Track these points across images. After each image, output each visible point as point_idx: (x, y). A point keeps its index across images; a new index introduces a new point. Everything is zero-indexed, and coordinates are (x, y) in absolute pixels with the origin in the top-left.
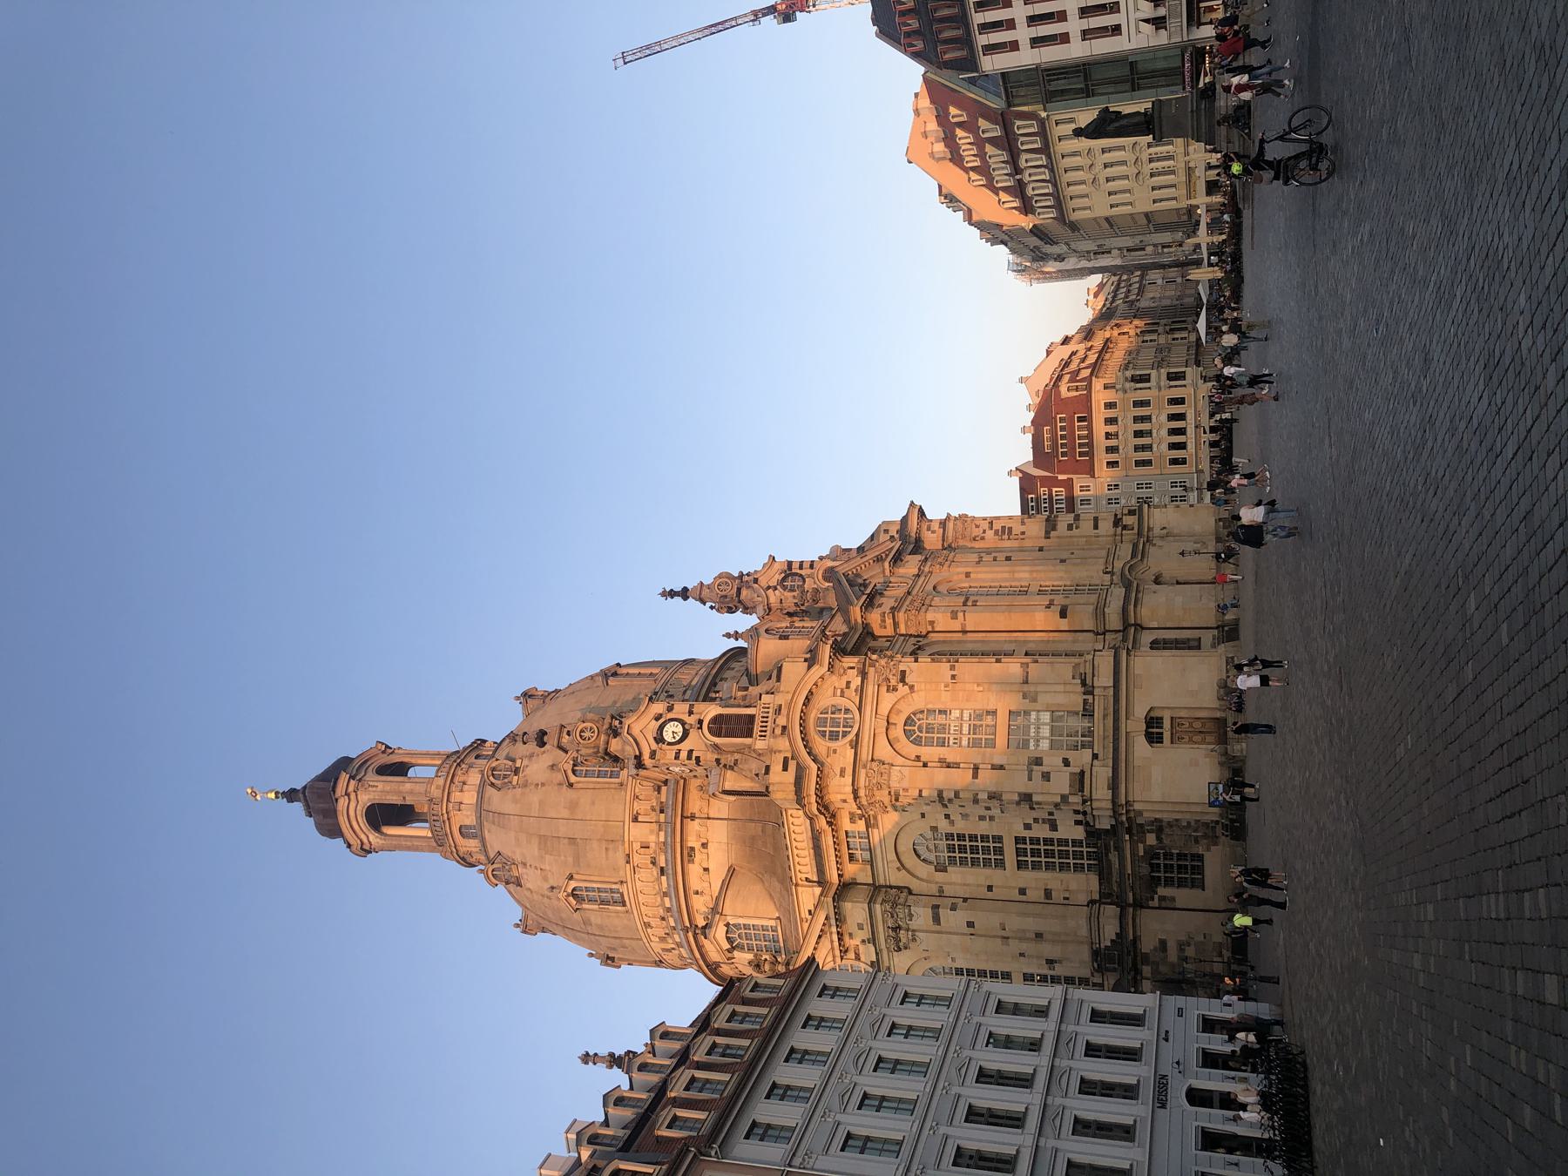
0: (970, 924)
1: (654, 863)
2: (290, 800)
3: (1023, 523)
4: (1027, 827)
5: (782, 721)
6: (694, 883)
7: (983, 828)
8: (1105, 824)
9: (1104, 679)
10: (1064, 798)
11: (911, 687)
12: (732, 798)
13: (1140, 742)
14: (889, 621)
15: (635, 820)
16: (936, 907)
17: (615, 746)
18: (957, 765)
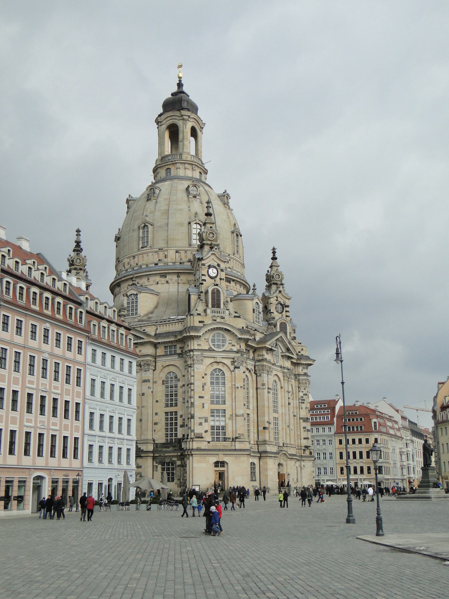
0: (143, 394)
1: (159, 260)
3: (306, 408)
4: (181, 416)
5: (218, 320)
6: (152, 279)
7: (180, 399)
8: (183, 446)
9: (238, 446)
10: (194, 430)
11: (233, 371)
12: (187, 298)
13: (215, 459)
14: (260, 358)
15: (177, 252)
16: (148, 381)
17: (207, 248)
18: (203, 390)
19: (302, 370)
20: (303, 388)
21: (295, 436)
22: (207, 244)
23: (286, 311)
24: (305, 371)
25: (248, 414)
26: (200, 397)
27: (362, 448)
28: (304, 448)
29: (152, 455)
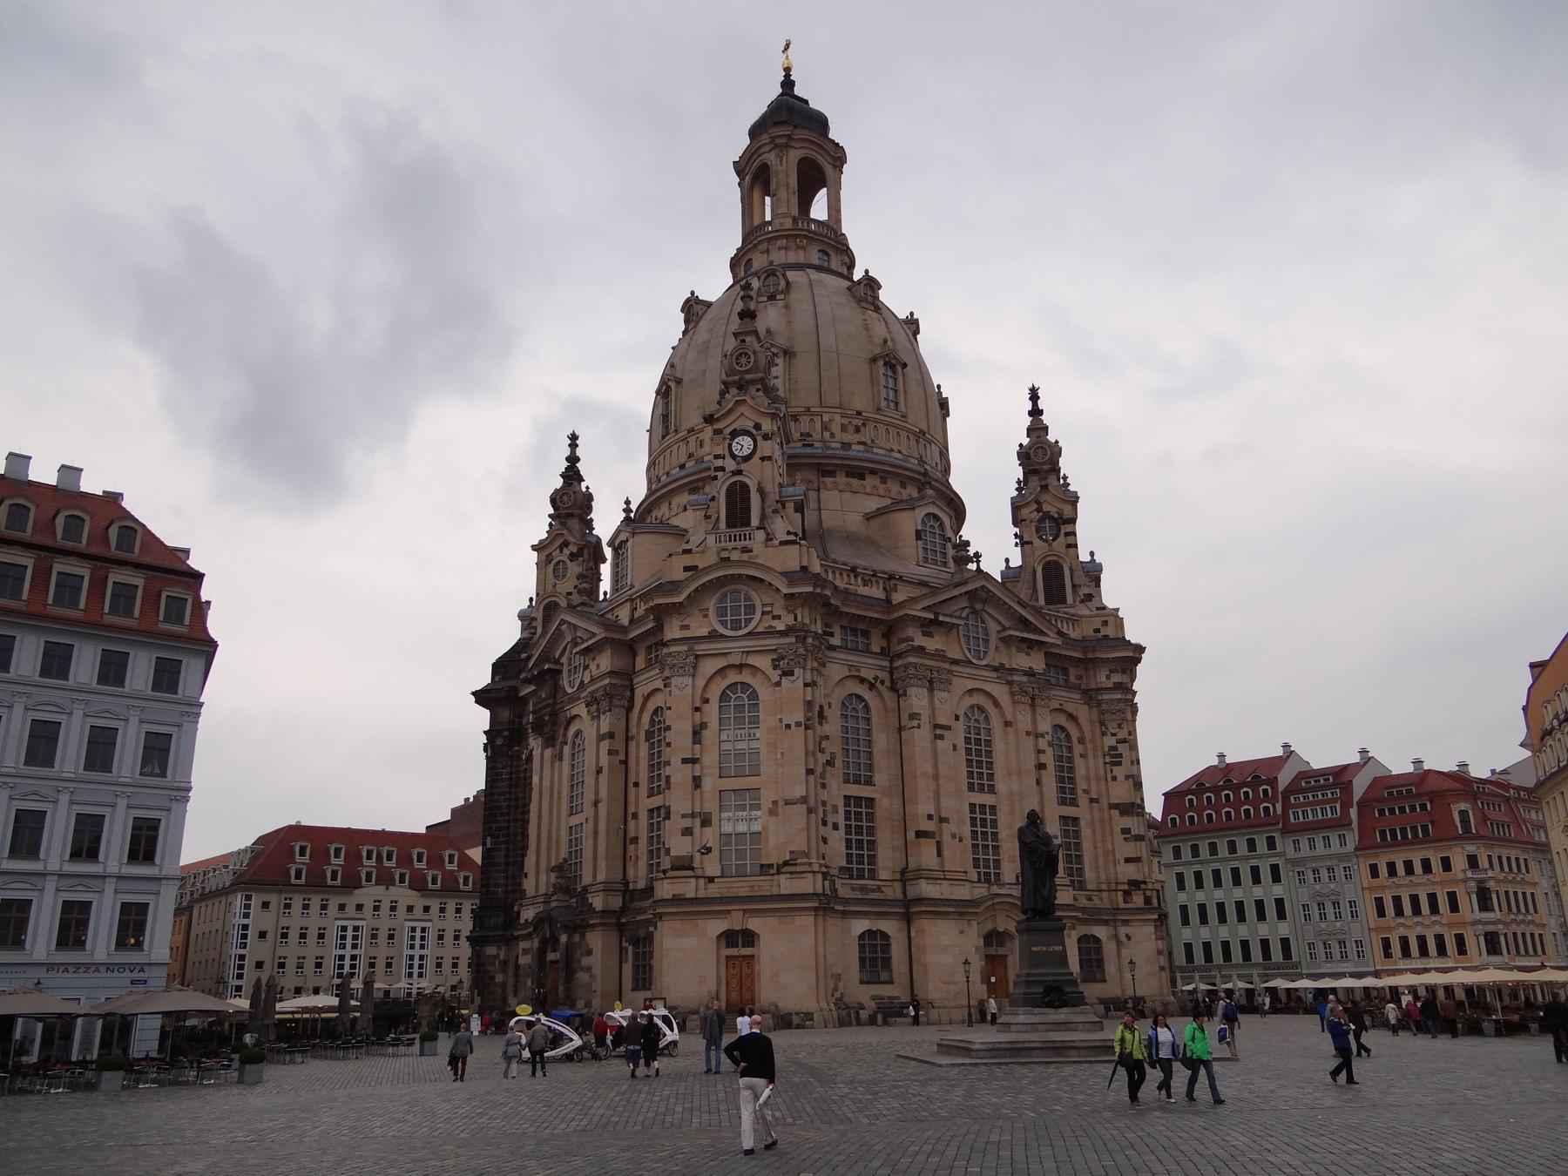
1: (690, 456)
2: (783, 85)
3: (1127, 777)
5: (735, 556)
9: (786, 885)
10: (668, 851)
11: (778, 684)
19: (1108, 677)
20: (1115, 724)
21: (1096, 855)
22: (734, 382)
23: (1067, 534)
24: (1116, 678)
26: (685, 761)
27: (1434, 883)
28: (1126, 887)
29: (613, 921)
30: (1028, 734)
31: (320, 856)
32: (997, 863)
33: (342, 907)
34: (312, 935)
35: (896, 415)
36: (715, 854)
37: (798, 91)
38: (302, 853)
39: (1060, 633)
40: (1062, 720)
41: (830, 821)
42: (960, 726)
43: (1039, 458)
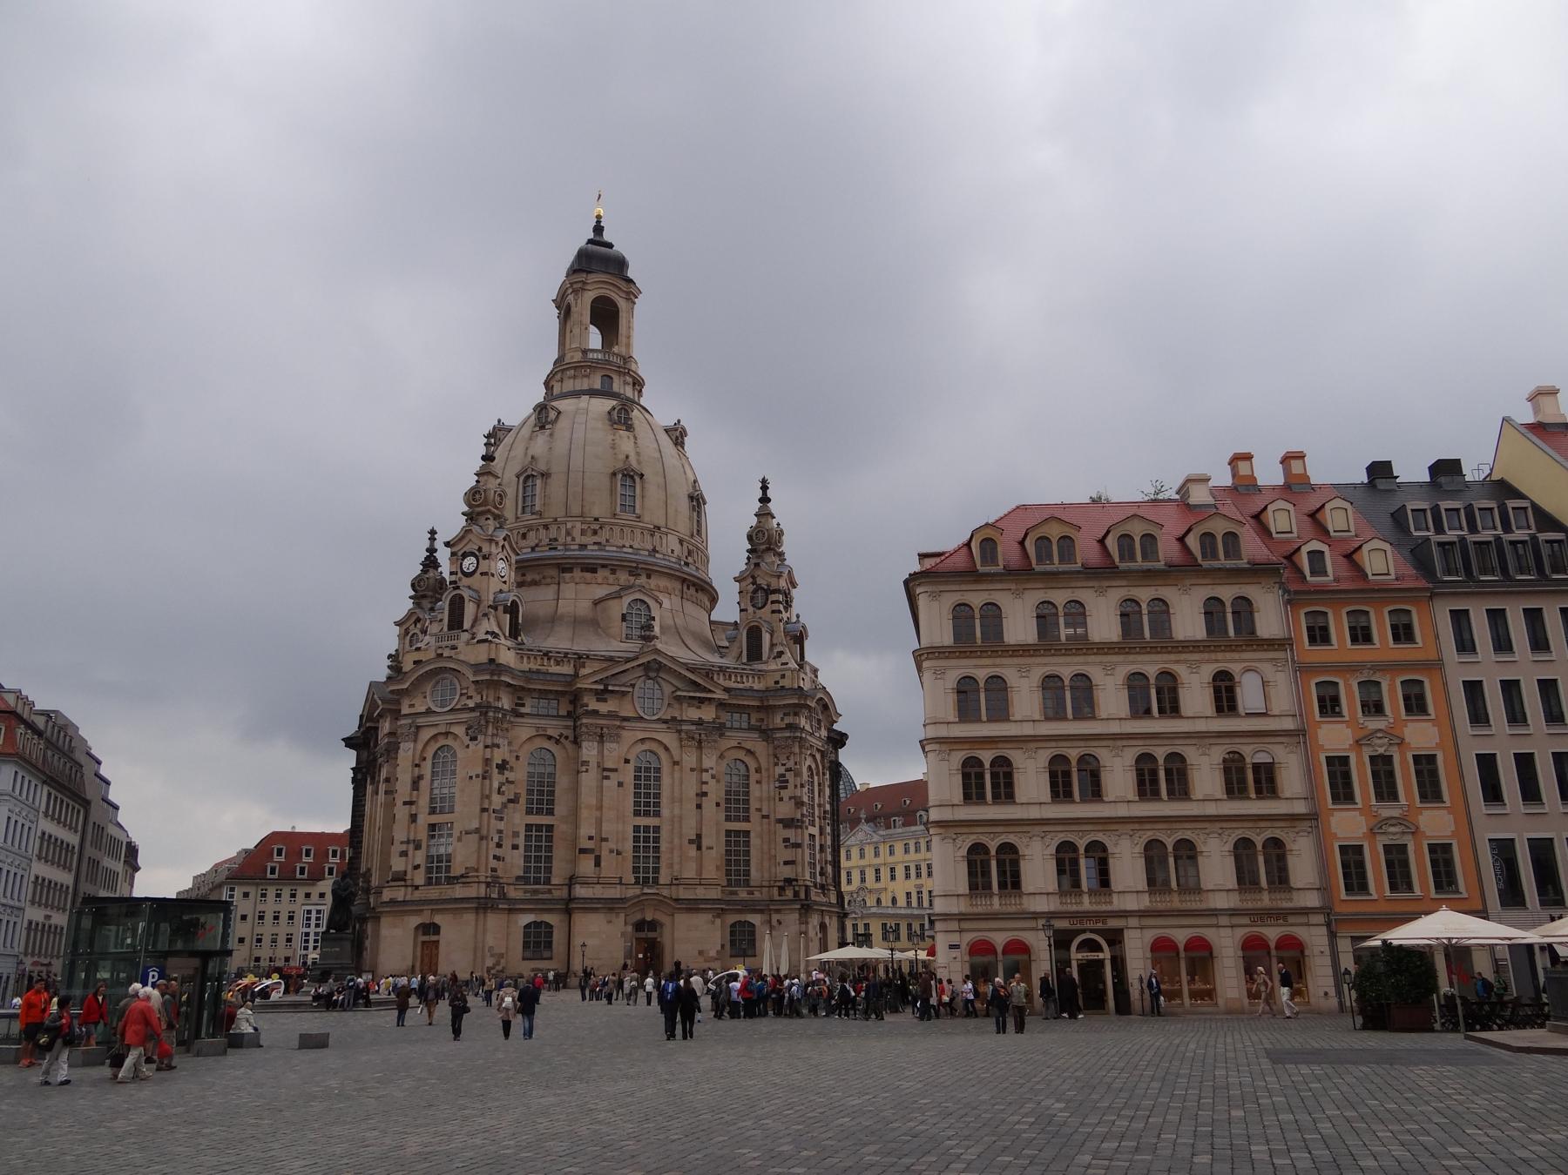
9: (459, 891)
25: (550, 828)
26: (405, 803)
30: (692, 770)
31: (295, 854)
32: (657, 870)
33: (308, 895)
34: (284, 917)
35: (631, 517)
36: (422, 870)
37: (607, 237)
38: (279, 854)
39: (727, 690)
40: (741, 755)
41: (507, 843)
42: (631, 767)
43: (764, 542)
